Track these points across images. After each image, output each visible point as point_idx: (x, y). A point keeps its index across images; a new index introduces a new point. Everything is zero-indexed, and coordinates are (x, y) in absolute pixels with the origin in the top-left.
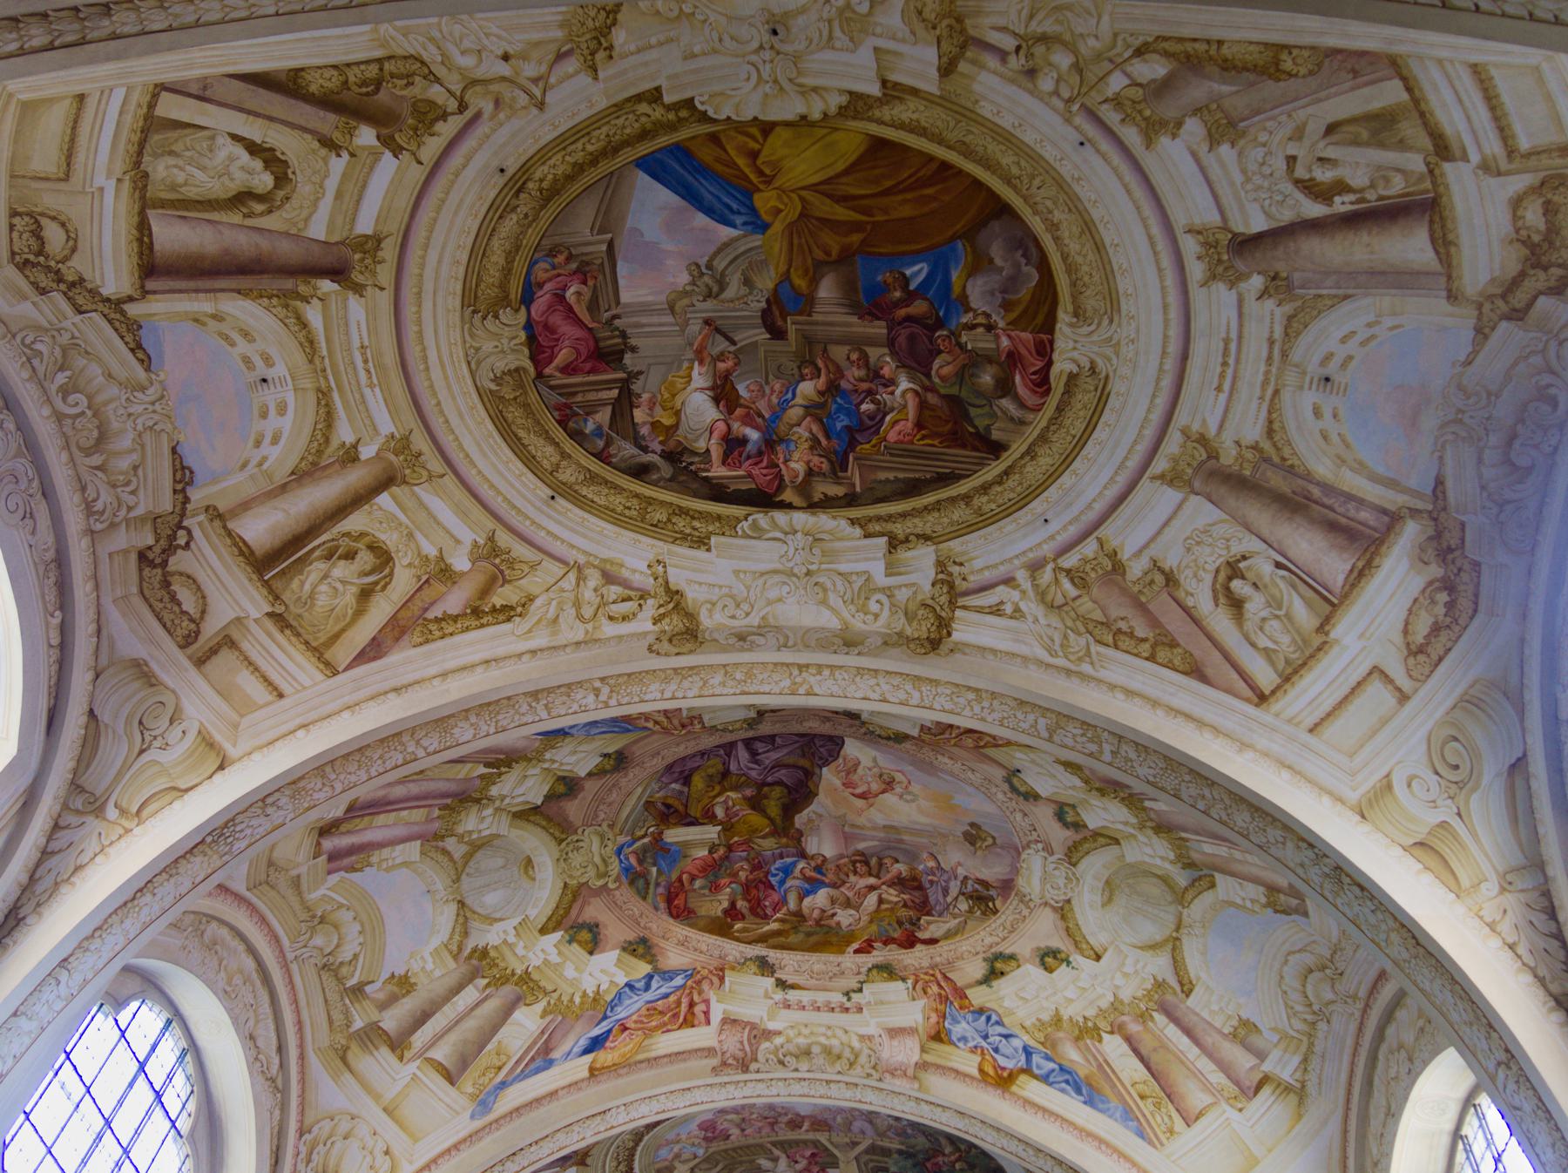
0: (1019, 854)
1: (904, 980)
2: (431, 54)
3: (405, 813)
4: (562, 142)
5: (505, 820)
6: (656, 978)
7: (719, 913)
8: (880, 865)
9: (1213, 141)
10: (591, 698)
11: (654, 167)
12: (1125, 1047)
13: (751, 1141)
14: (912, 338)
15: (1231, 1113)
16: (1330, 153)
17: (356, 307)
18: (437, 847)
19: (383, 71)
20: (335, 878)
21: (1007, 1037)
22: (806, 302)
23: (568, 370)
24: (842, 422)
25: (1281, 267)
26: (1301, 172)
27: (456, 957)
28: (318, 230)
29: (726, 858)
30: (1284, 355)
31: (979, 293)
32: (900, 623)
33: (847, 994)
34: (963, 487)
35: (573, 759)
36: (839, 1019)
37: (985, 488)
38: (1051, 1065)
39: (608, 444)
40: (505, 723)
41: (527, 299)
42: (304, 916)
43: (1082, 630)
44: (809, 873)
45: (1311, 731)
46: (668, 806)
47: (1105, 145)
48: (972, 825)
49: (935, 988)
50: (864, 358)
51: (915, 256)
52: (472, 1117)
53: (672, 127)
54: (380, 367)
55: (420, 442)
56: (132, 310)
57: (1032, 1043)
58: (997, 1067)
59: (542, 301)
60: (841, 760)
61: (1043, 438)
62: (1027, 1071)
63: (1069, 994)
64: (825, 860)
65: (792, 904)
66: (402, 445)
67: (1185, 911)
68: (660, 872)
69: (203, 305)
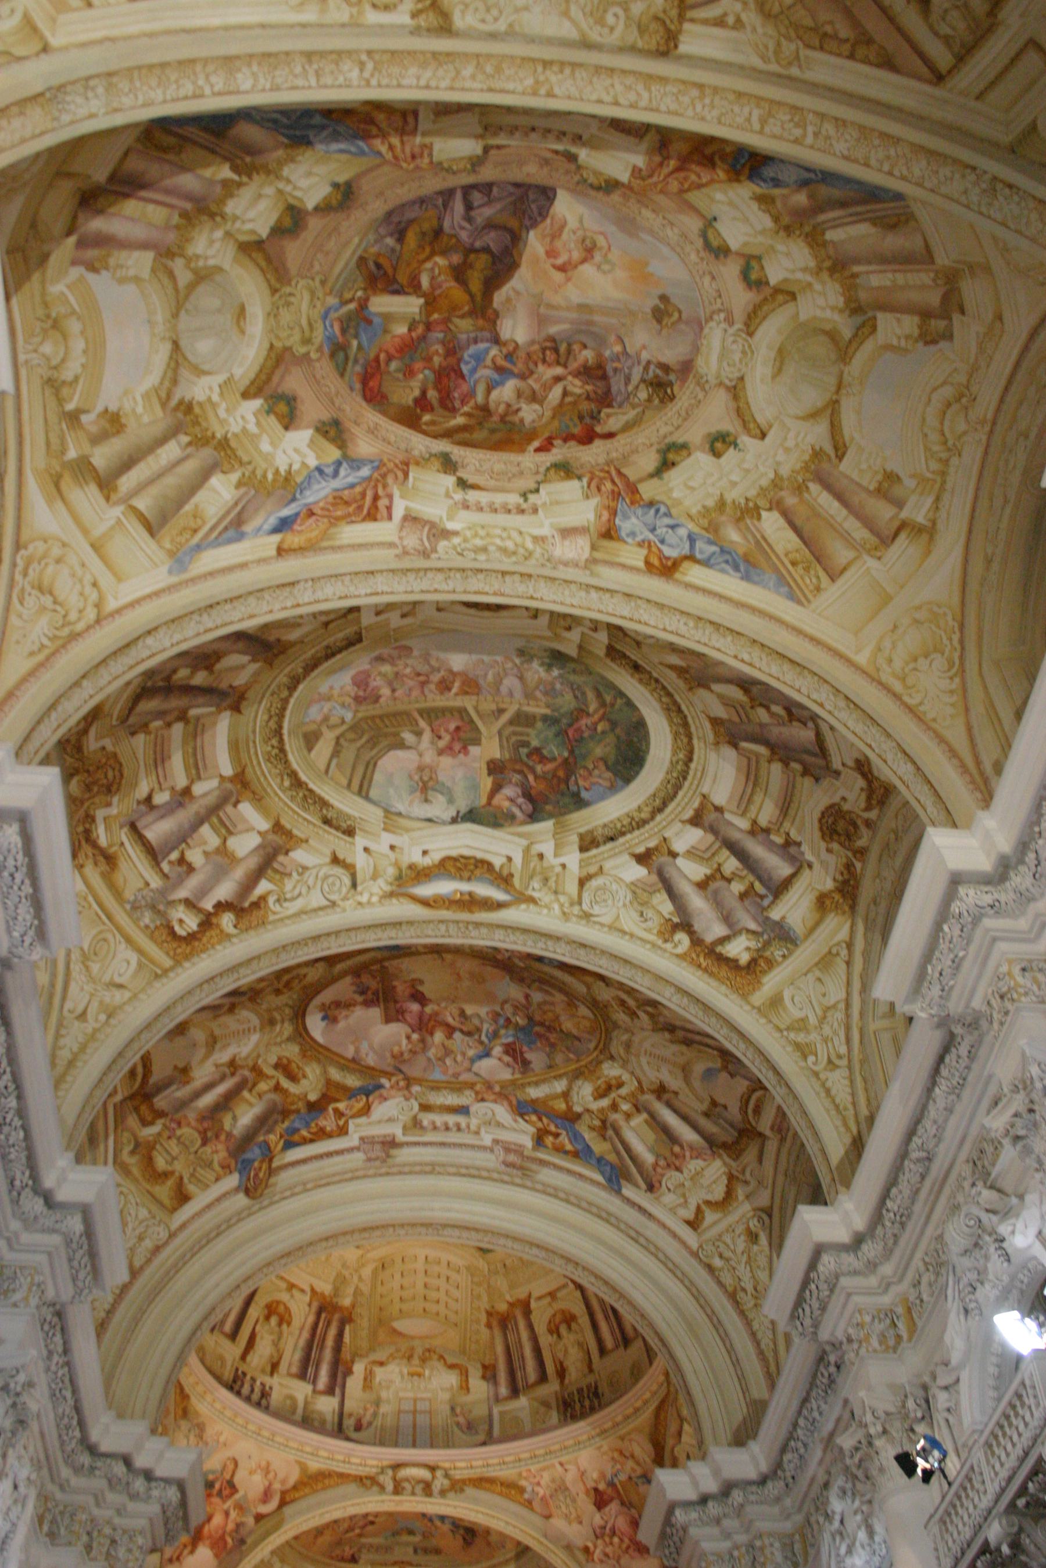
0: (702, 329)
1: (580, 478)
3: (151, 207)
5: (231, 250)
6: (345, 465)
7: (411, 403)
8: (569, 351)
10: (355, 74)
12: (782, 522)
13: (400, 707)
15: (871, 563)
18: (166, 267)
20: (77, 272)
21: (673, 527)
27: (164, 405)
29: (423, 338)
32: (633, 37)
33: (524, 495)
35: (303, 183)
36: (515, 521)
38: (714, 548)
40: (279, 80)
42: (40, 312)
43: (793, 34)
44: (501, 362)
45: (977, 98)
46: (378, 266)
48: (664, 298)
49: (609, 485)
52: (170, 572)
57: (696, 530)
58: (662, 557)
60: (548, 221)
62: (691, 558)
63: (734, 477)
64: (517, 346)
65: (480, 398)
67: (846, 370)
68: (360, 347)
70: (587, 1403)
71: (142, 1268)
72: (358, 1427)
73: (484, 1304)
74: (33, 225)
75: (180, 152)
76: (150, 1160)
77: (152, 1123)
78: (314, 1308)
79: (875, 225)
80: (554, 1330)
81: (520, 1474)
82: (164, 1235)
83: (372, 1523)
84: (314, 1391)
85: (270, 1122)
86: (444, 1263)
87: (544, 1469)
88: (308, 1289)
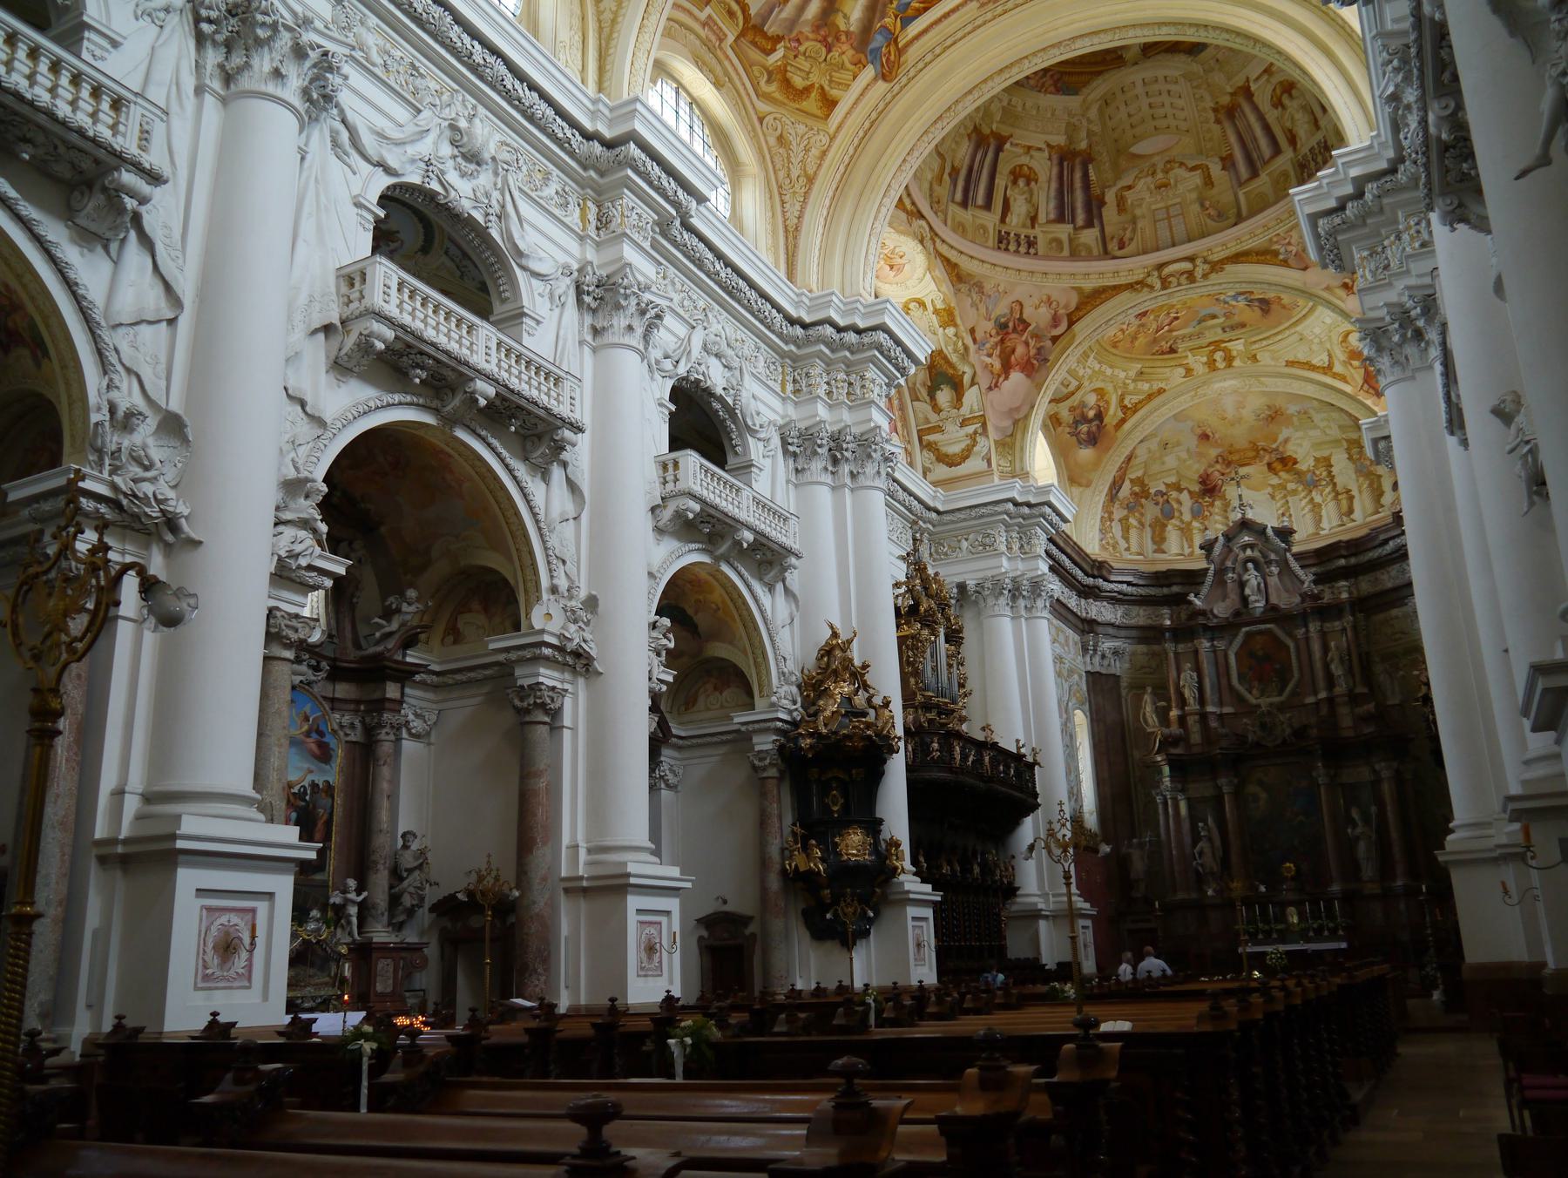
70: (1320, 159)
71: (815, 173)
72: (1122, 246)
73: (1209, 104)
76: (787, 84)
77: (773, 50)
78: (1055, 161)
80: (1278, 104)
81: (1271, 239)
82: (826, 140)
83: (1177, 318)
84: (1075, 229)
85: (880, 7)
86: (1161, 79)
87: (1291, 230)
88: (1044, 146)
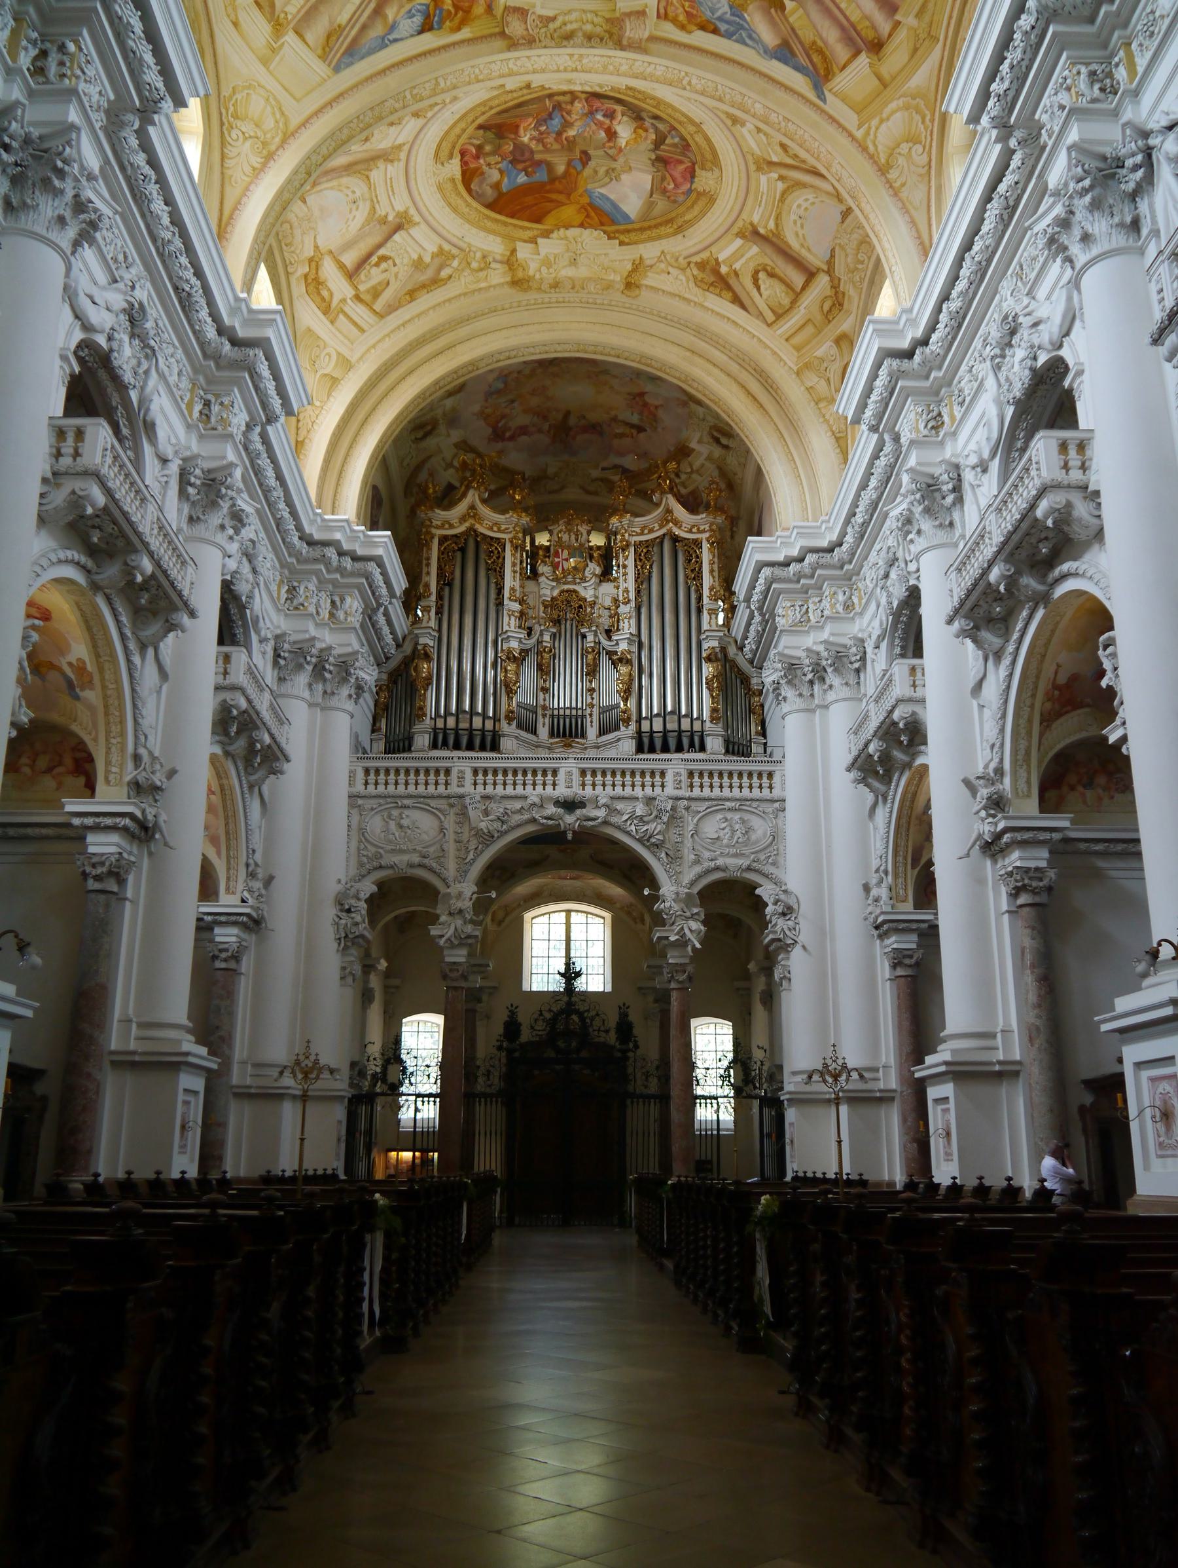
2: (691, 284)
4: (659, 238)
9: (420, 258)
10: (694, 81)
11: (626, 217)
14: (523, 154)
16: (385, 275)
17: (756, 219)
19: (709, 287)
22: (569, 164)
23: (681, 162)
24: (556, 122)
25: (384, 227)
26: (390, 262)
28: (755, 249)
30: (372, 201)
31: (495, 175)
34: (494, 111)
37: (484, 113)
39: (669, 132)
41: (690, 191)
47: (455, 240)
50: (544, 145)
51: (522, 185)
53: (618, 231)
54: (757, 198)
55: (752, 167)
56: (825, 268)
59: (686, 187)
61: (459, 136)
66: (759, 169)
69: (804, 253)
74: (916, 50)
75: (814, 43)
79: (339, 26)
